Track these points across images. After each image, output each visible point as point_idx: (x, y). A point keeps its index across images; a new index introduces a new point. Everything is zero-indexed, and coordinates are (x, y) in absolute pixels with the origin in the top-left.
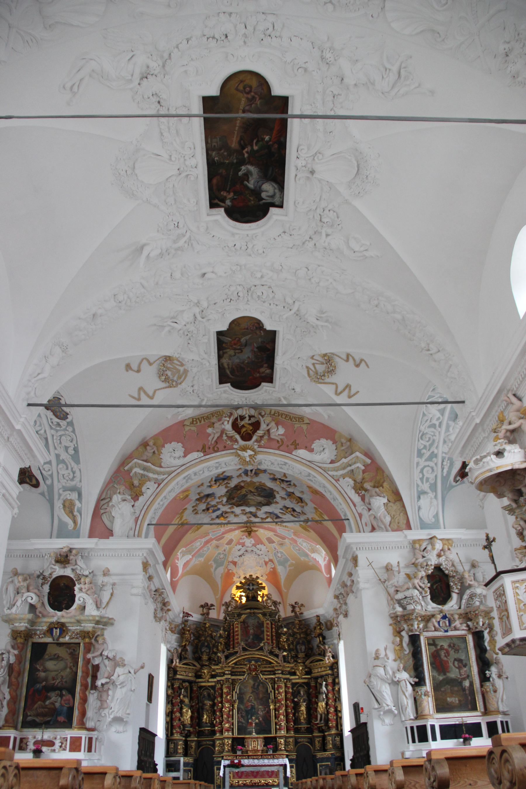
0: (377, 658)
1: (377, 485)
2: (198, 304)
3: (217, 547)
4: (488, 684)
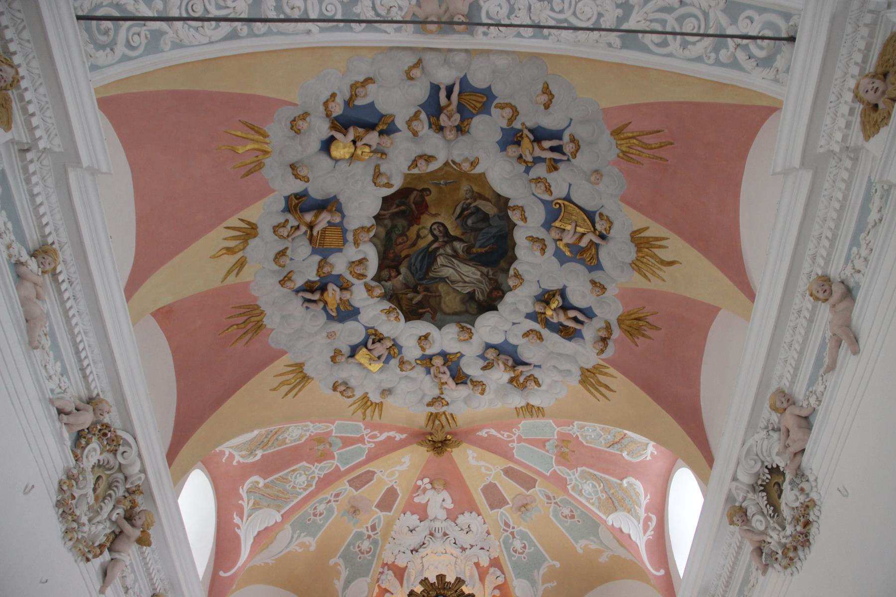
3: (355, 511)
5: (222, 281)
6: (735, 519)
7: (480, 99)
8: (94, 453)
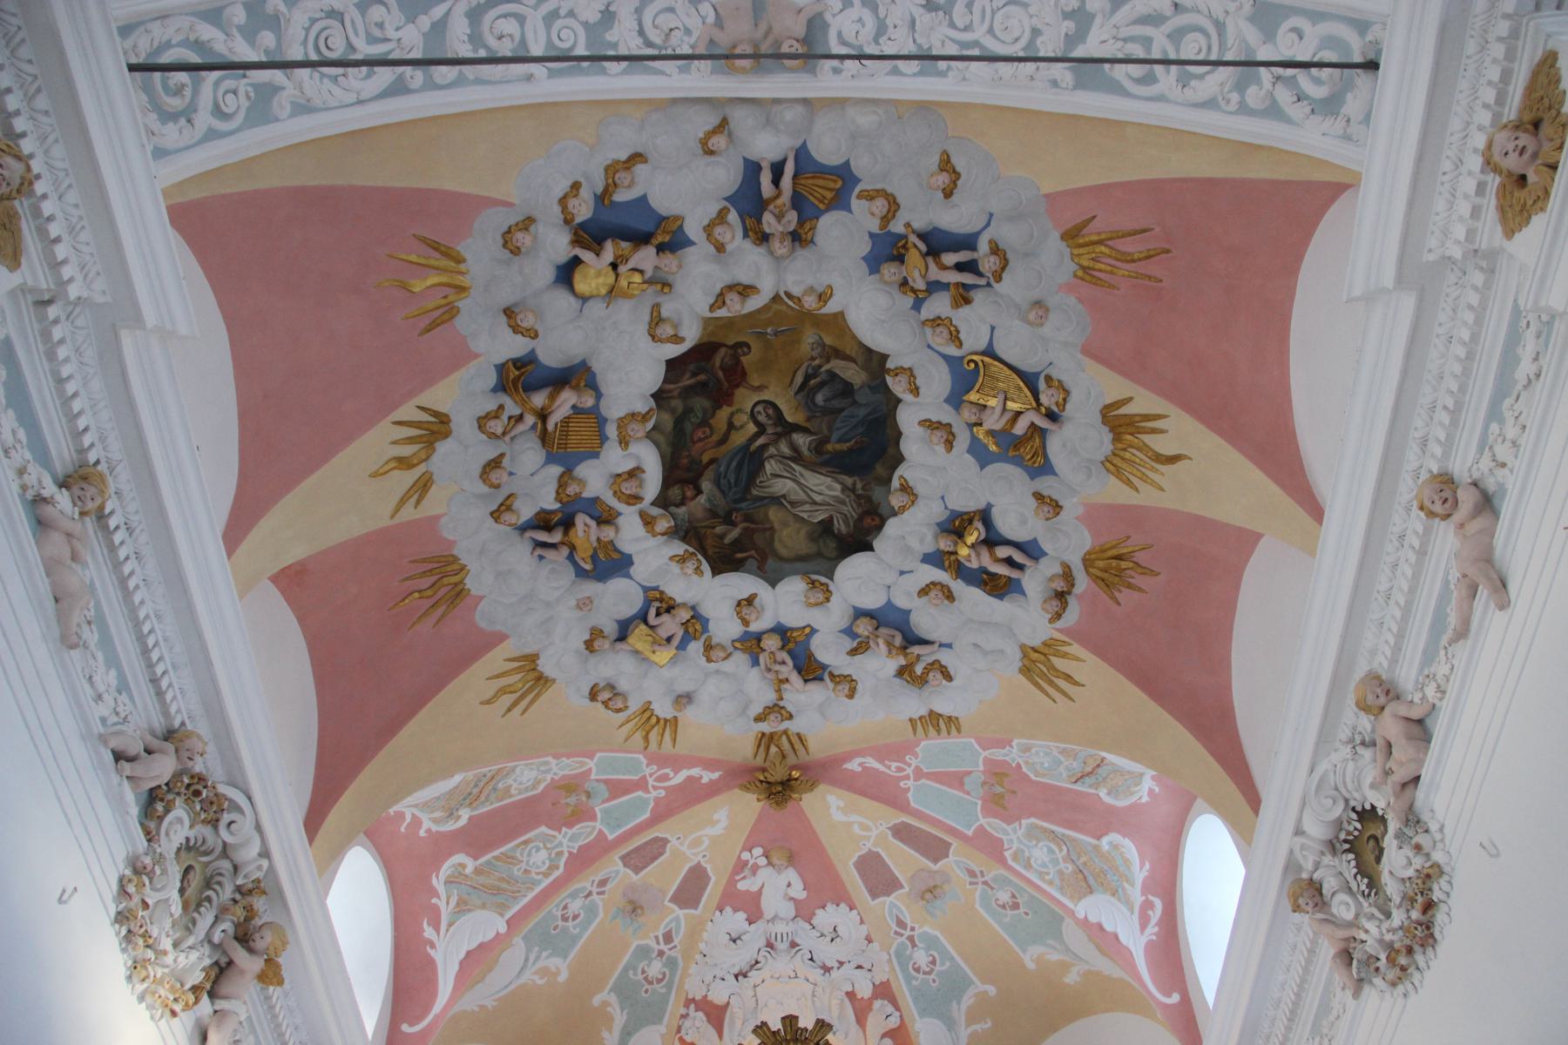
3: (634, 908)
5: (392, 517)
6: (1301, 901)
7: (832, 185)
8: (179, 825)
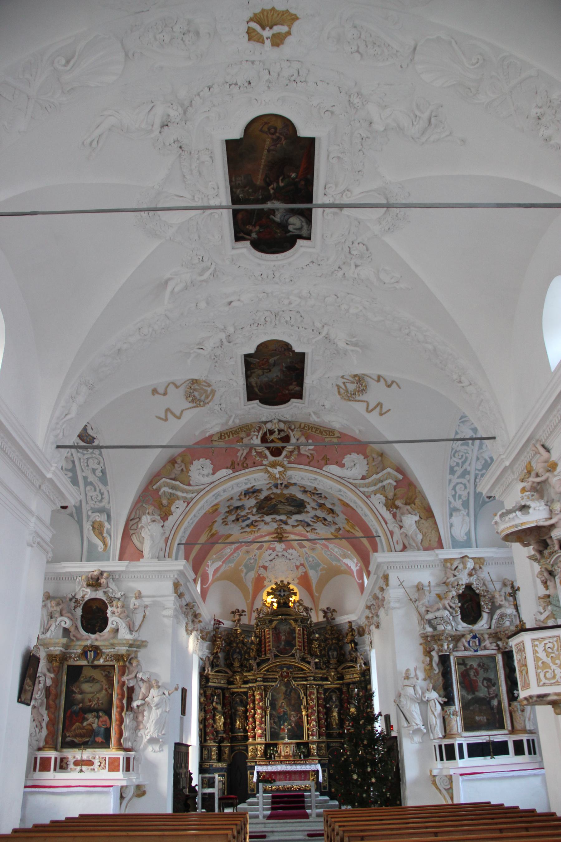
0: (407, 677)
1: (408, 501)
2: (224, 330)
3: (248, 552)
4: (515, 703)
